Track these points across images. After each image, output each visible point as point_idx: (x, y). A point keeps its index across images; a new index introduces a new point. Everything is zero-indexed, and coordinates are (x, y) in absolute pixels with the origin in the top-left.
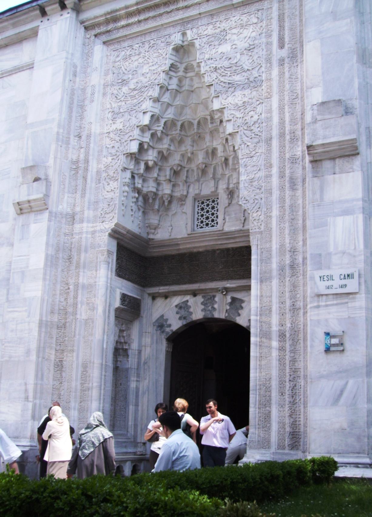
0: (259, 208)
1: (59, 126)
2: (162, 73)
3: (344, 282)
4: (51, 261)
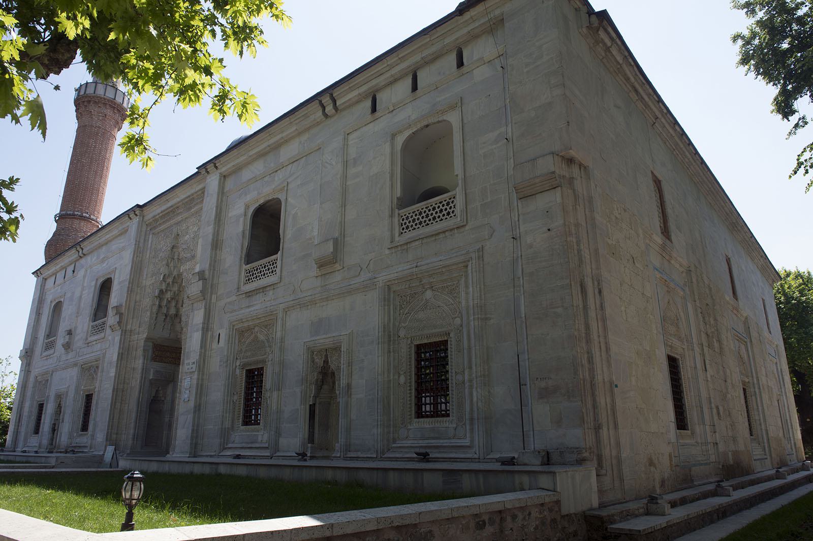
1: (129, 284)
3: (192, 366)
4: (121, 356)
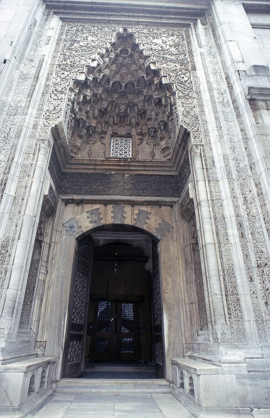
0: (198, 129)
2: (108, 43)
